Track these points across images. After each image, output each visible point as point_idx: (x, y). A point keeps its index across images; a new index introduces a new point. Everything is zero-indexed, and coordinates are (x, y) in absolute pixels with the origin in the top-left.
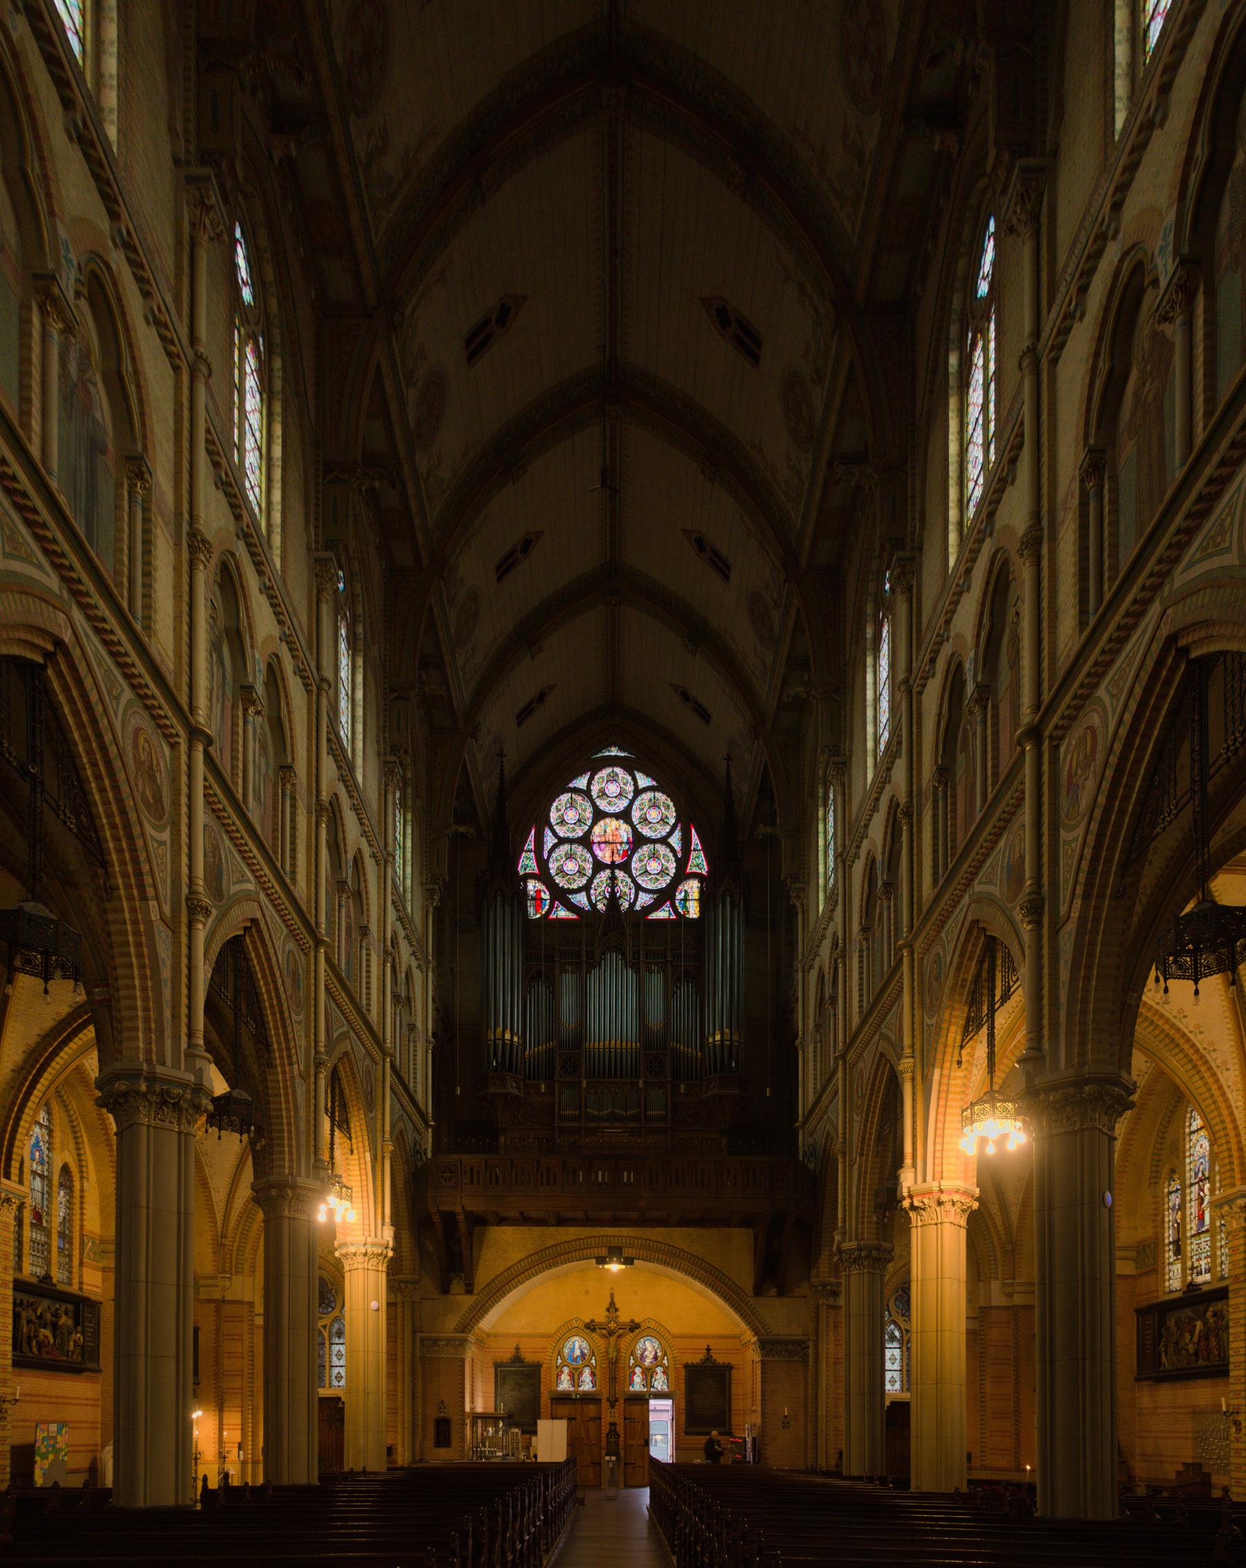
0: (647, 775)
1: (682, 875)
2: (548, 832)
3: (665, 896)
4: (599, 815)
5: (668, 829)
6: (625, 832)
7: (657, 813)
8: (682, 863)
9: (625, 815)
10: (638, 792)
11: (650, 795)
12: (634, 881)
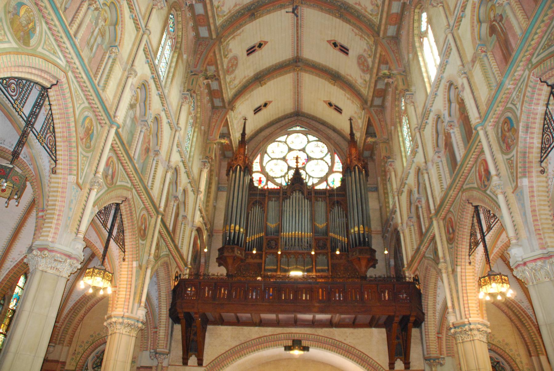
0: (314, 136)
1: (331, 171)
3: (325, 179)
7: (318, 148)
10: (309, 142)
11: (316, 143)
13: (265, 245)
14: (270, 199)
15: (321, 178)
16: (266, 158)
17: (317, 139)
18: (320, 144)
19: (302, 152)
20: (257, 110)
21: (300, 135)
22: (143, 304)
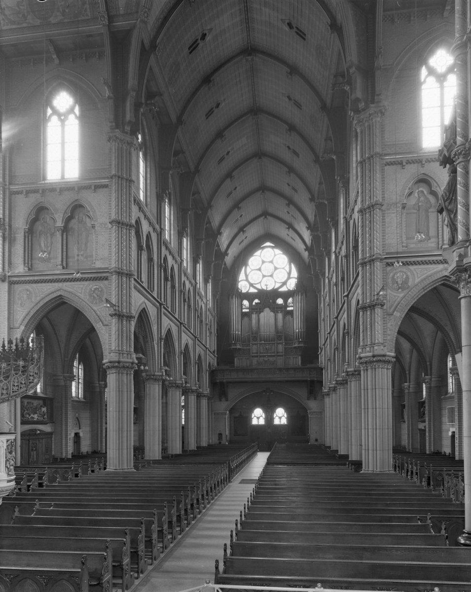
1: (289, 278)
3: (284, 283)
4: (263, 262)
5: (285, 265)
6: (271, 267)
8: (289, 273)
20: (240, 244)
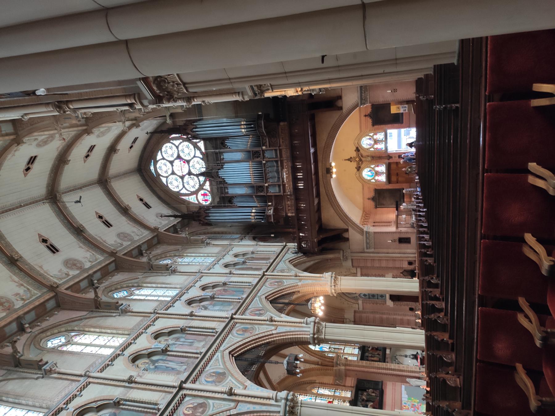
2: (182, 192)
4: (173, 173)
5: (173, 146)
6: (177, 163)
9: (171, 163)
10: (163, 159)
11: (163, 154)
12: (192, 158)
13: (262, 194)
14: (227, 193)
15: (194, 147)
16: (184, 191)
17: (160, 152)
18: (164, 149)
19: (174, 164)
20: (148, 206)
21: (158, 166)
22: (321, 275)
